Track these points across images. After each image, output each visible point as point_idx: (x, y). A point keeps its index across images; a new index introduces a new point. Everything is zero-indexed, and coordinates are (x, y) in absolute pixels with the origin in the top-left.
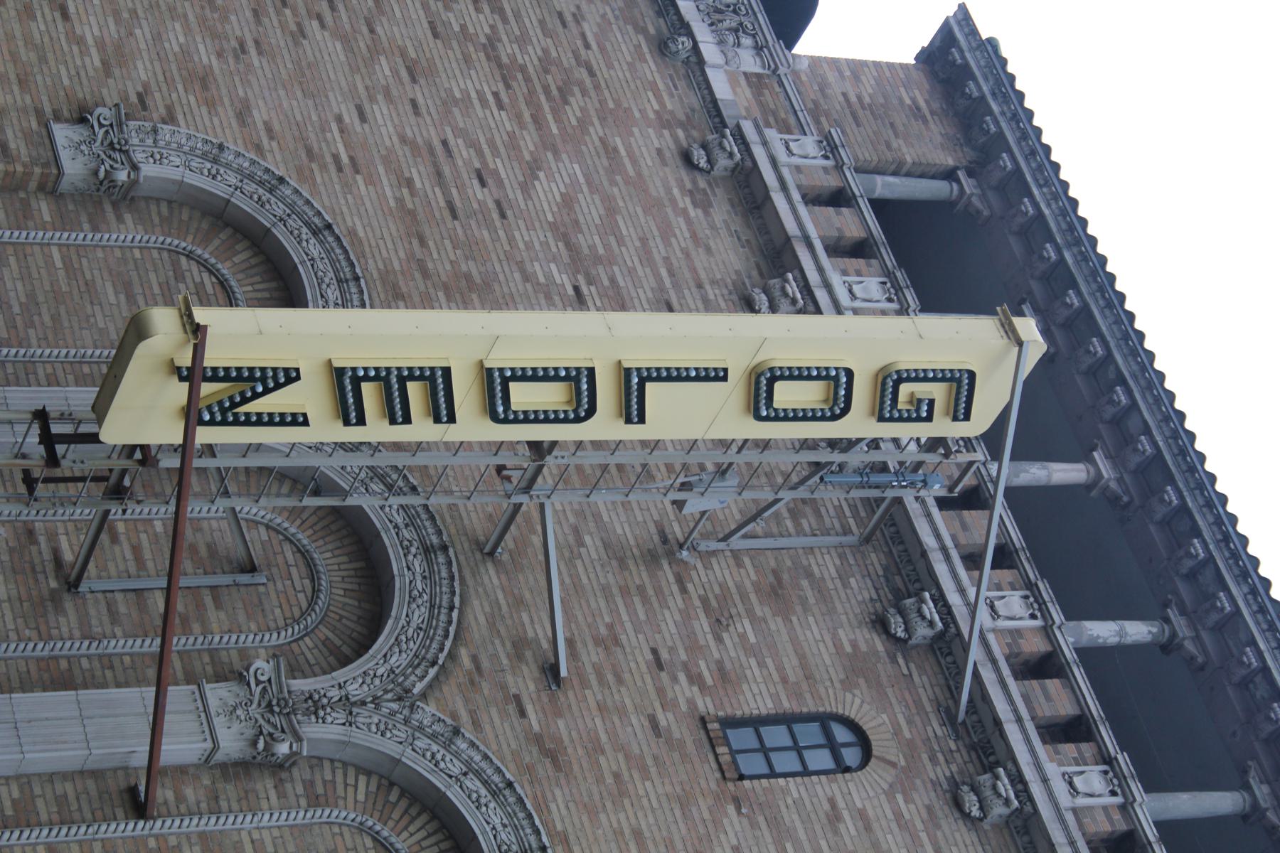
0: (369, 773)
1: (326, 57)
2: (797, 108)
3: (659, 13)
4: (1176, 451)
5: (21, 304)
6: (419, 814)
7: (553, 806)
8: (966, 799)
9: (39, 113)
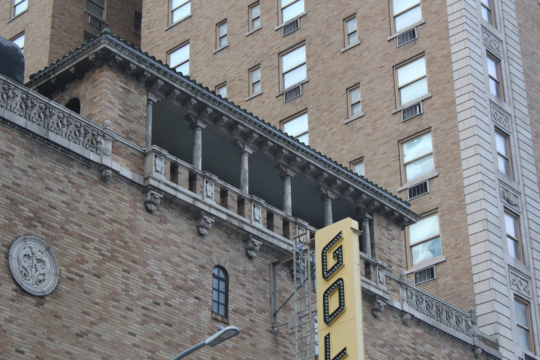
1: (110, 332)
2: (128, 144)
3: (89, 168)
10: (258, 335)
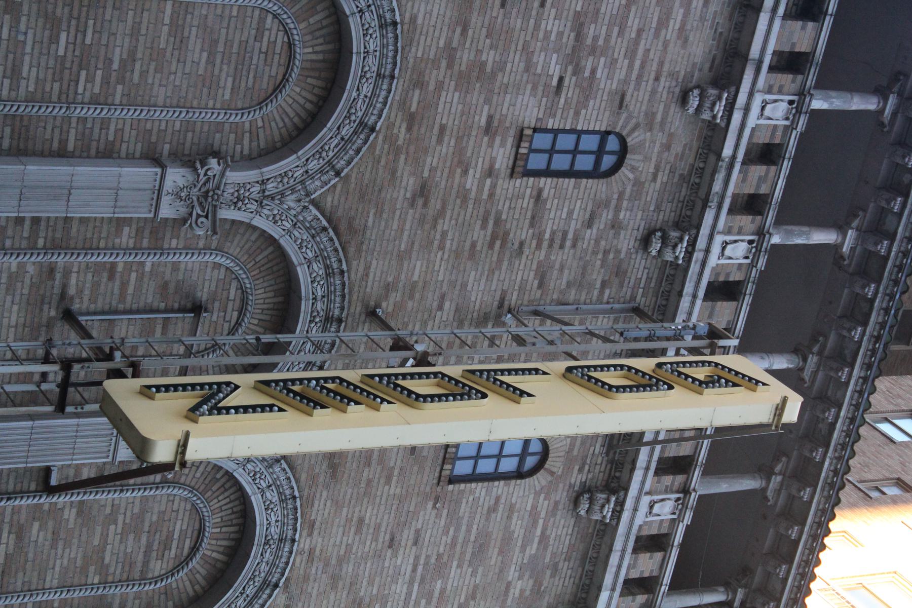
4: (898, 263)
5: (121, 60)
6: (230, 487)
7: (316, 502)
8: (582, 506)
10: (494, 265)
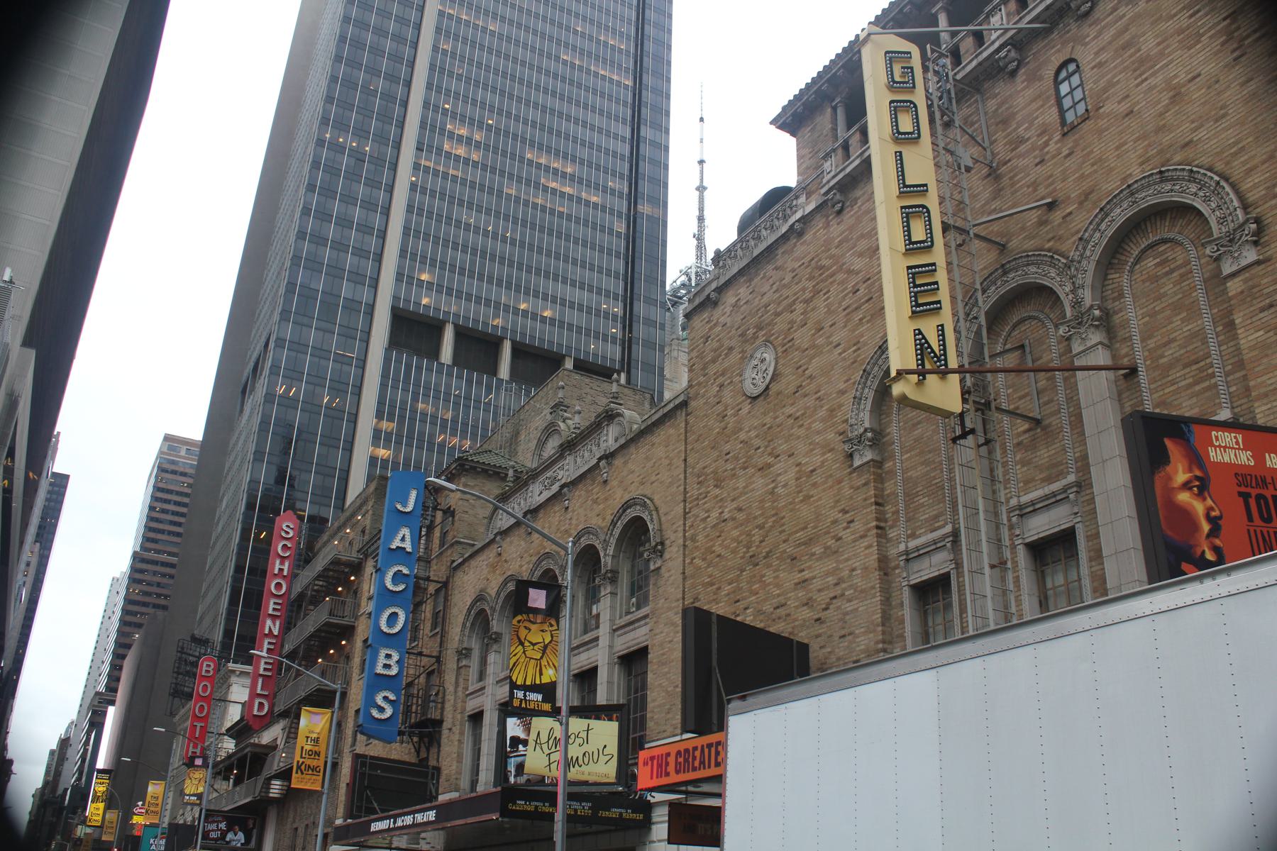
0: (1106, 275)
9: (851, 473)
